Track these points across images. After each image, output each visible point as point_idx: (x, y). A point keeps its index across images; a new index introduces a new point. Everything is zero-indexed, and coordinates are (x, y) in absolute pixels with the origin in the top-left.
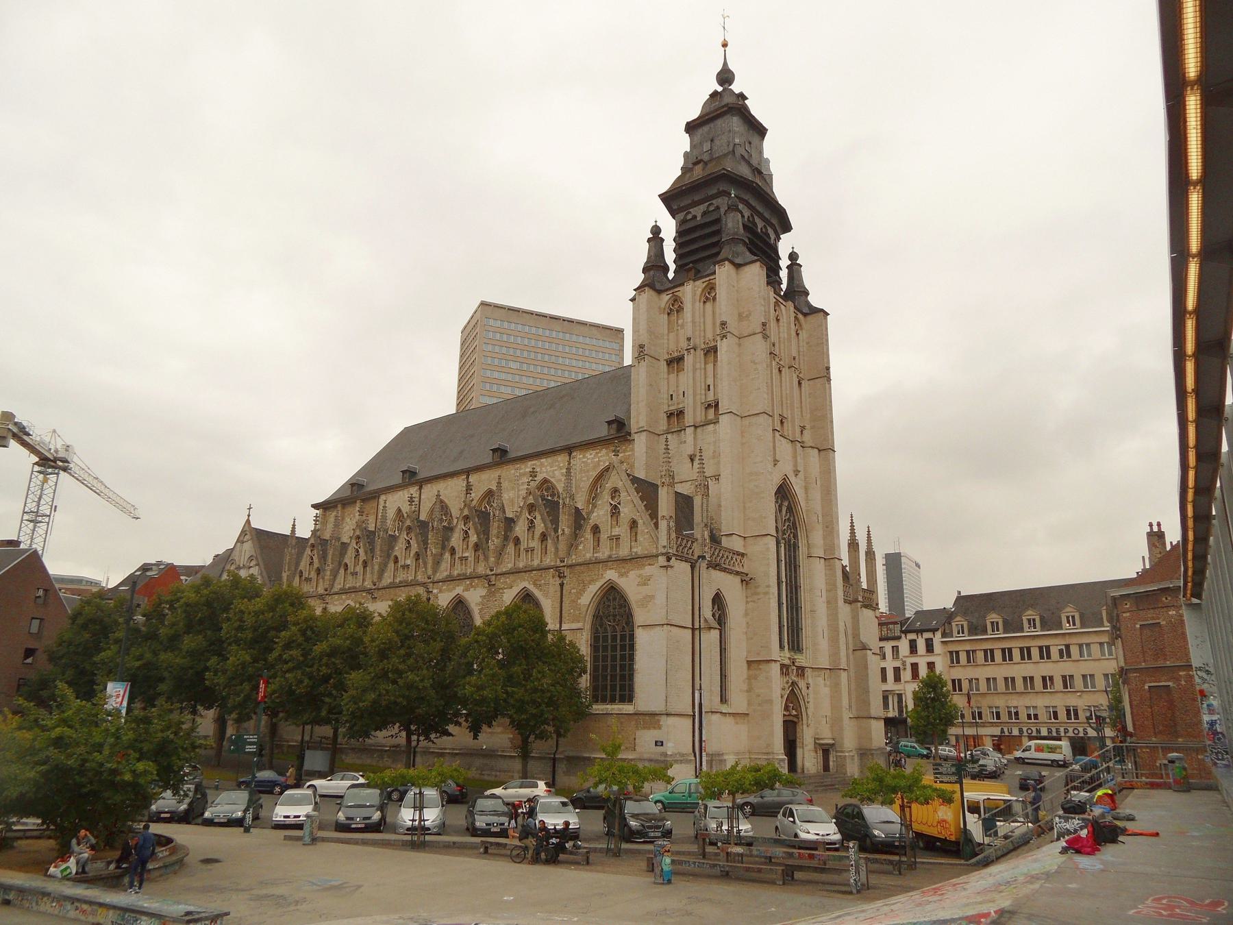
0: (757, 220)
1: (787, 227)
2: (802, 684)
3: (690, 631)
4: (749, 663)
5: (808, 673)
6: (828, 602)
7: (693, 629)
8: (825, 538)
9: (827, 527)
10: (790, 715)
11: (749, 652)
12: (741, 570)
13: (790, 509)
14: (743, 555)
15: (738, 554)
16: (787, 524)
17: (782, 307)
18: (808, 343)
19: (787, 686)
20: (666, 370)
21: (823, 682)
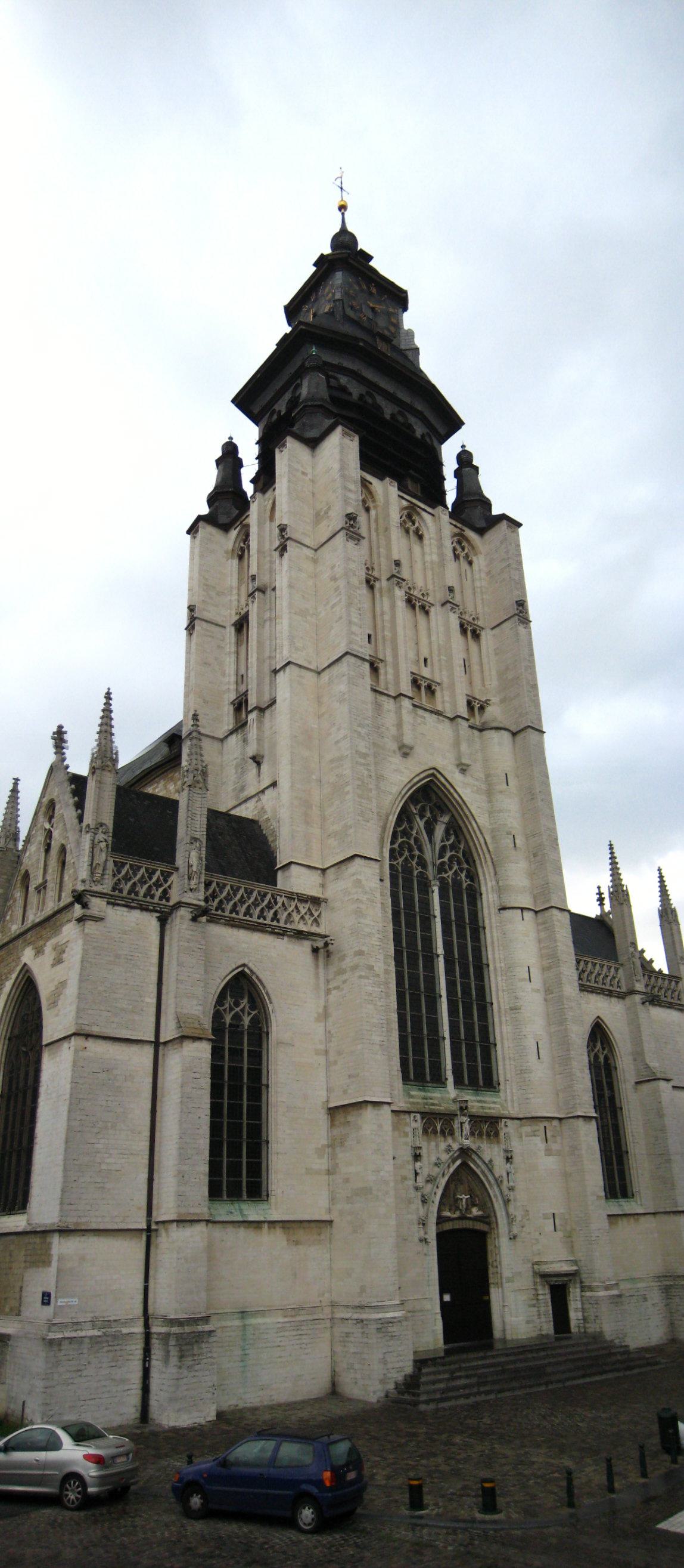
0: (380, 401)
1: (453, 423)
2: (490, 1152)
3: (149, 1051)
4: (333, 1112)
5: (508, 1129)
6: (548, 991)
7: (157, 1044)
8: (531, 875)
9: (535, 855)
10: (463, 1218)
11: (329, 1090)
12: (314, 929)
13: (456, 829)
14: (316, 901)
15: (303, 899)
16: (448, 854)
17: (424, 514)
18: (488, 573)
19: (445, 1157)
20: (233, 639)
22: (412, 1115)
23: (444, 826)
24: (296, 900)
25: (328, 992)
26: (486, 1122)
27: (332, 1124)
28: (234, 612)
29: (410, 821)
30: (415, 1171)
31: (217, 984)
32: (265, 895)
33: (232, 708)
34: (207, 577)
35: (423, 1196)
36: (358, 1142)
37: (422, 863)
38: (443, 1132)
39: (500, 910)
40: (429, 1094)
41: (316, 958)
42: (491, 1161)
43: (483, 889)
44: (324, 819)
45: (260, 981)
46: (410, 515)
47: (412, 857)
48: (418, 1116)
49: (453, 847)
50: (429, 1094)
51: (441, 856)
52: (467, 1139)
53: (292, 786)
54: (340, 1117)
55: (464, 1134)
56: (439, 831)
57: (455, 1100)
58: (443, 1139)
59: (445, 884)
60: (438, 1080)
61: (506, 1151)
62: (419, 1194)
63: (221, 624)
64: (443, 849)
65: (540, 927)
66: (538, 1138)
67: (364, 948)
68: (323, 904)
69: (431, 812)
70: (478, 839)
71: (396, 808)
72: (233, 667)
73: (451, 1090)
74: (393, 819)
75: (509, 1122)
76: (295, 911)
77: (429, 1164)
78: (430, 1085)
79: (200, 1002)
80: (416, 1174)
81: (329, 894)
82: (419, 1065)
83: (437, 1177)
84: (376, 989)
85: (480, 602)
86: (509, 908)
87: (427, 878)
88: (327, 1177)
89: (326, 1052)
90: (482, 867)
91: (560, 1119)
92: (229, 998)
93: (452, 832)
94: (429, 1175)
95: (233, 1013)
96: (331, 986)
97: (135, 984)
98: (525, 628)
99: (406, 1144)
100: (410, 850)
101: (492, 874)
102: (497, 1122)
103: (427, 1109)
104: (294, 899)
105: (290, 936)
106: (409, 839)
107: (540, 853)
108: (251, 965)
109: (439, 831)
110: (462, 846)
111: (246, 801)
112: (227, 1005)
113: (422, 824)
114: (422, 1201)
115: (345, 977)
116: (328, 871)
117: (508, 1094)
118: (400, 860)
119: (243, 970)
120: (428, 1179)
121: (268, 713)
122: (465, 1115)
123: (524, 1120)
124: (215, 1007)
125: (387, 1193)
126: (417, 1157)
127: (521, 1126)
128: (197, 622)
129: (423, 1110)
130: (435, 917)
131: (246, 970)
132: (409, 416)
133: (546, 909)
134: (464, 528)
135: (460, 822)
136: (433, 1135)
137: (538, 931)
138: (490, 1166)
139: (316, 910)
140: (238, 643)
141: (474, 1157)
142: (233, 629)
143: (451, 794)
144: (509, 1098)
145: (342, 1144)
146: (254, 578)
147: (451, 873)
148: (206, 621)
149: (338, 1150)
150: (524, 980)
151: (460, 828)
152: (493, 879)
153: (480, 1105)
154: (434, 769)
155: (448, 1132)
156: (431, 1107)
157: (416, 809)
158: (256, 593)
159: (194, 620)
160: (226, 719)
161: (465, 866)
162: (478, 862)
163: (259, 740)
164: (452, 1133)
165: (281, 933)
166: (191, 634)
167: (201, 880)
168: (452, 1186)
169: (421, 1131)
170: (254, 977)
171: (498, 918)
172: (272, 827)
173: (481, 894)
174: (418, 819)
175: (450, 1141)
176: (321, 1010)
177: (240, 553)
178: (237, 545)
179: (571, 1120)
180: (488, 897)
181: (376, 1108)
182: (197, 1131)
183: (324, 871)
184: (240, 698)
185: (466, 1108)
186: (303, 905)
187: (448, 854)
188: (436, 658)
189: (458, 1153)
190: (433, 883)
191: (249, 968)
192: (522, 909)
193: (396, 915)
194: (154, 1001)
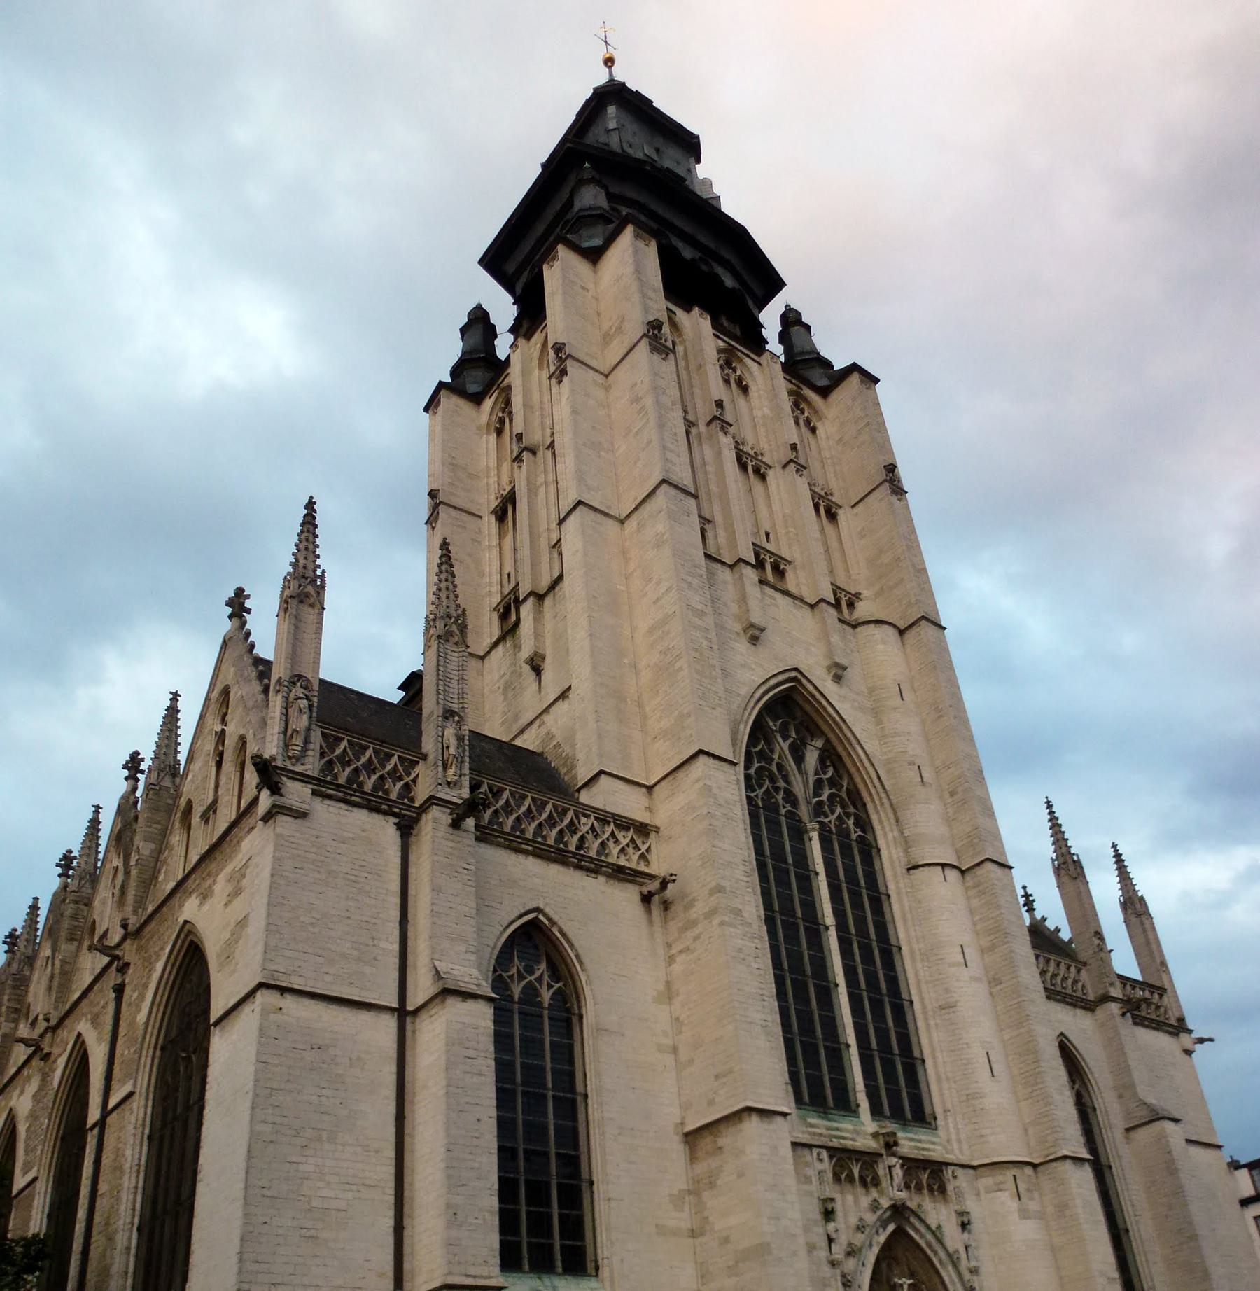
1: (772, 283)
2: (938, 1214)
4: (692, 1138)
5: (959, 1182)
7: (404, 1014)
11: (685, 1106)
13: (830, 756)
14: (643, 830)
19: (871, 1218)
21: (1013, 1205)
22: (815, 1151)
23: (816, 754)
24: (612, 824)
25: (671, 960)
26: (925, 1169)
27: (693, 1158)
28: (493, 497)
29: (769, 742)
30: (829, 1236)
31: (497, 936)
32: (565, 811)
33: (495, 616)
34: (454, 455)
35: (843, 1276)
36: (741, 1175)
37: (790, 797)
38: (864, 1183)
39: (909, 869)
40: (836, 1125)
41: (649, 911)
42: (939, 1227)
43: (881, 843)
44: (644, 717)
45: (563, 934)
46: (728, 361)
47: (777, 789)
48: (825, 1154)
49: (833, 783)
50: (836, 1125)
51: (817, 793)
52: (901, 1191)
53: (594, 668)
54: (706, 1143)
55: (895, 1185)
56: (811, 758)
57: (875, 1135)
58: (864, 1191)
59: (827, 831)
60: (845, 1105)
61: (960, 1214)
62: (838, 1272)
63: (477, 513)
64: (819, 784)
65: (971, 893)
66: (1007, 1194)
67: (726, 884)
68: (653, 835)
69: (797, 733)
70: (868, 773)
71: (750, 714)
72: (496, 564)
73: (867, 1123)
74: (745, 730)
75: (959, 1172)
76: (611, 841)
77: (848, 1227)
78: (834, 1112)
79: (472, 949)
80: (830, 1240)
81: (659, 819)
82: (816, 1084)
83: (862, 1247)
84: (747, 943)
85: (833, 475)
86: (923, 866)
87: (800, 821)
88: (691, 1240)
89: (675, 1050)
90: (877, 812)
91: (1035, 1166)
92: (516, 959)
93: (828, 764)
94: (850, 1244)
95: (524, 983)
96: (673, 951)
97: (365, 918)
98: (900, 500)
99: (811, 1194)
100: (773, 780)
101: (893, 821)
102: (942, 1171)
103: (835, 1143)
104: (609, 823)
105: (609, 876)
106: (770, 764)
107: (960, 789)
108: (547, 910)
109: (811, 758)
110: (845, 784)
111: (522, 731)
112: (514, 971)
113: (785, 746)
114: (844, 1285)
115: (696, 931)
116: (657, 788)
117: (952, 1130)
118: (760, 792)
119: (537, 918)
120: (849, 1250)
121: (548, 601)
122: (894, 1155)
123: (982, 1169)
124: (495, 971)
125: (795, 1254)
126: (828, 1215)
127: (977, 1178)
128: (443, 512)
129: (831, 1144)
130: (817, 874)
131: (541, 917)
132: (715, 265)
133: (978, 864)
134: (801, 386)
135: (840, 749)
136: (848, 1186)
137: (968, 898)
138: (938, 1235)
139: (643, 843)
140: (501, 535)
141: (912, 1219)
142: (493, 518)
143: (825, 709)
144: (953, 1137)
145: (712, 1185)
146: (519, 437)
147: (833, 818)
148: (455, 508)
149: (706, 1195)
150: (957, 964)
151: (840, 758)
152: (894, 827)
153: (913, 1144)
154: (796, 669)
155: (870, 1181)
156: (842, 1141)
157: (775, 725)
158: (524, 453)
159: (437, 507)
160: (487, 630)
161: (852, 810)
162: (870, 806)
163: (538, 636)
164: (876, 1183)
165: (594, 868)
166: (433, 528)
167: (463, 772)
168: (884, 1266)
169: (830, 1175)
170: (555, 930)
171: (906, 881)
172: (564, 754)
173: (879, 850)
174: (780, 740)
175: (874, 1193)
176: (661, 987)
177: (498, 426)
178: (494, 417)
179: (1054, 1164)
180: (890, 853)
181: (766, 1120)
182: (476, 1142)
183: (650, 789)
184: (506, 599)
185: (896, 1144)
186: (623, 833)
187: (826, 793)
188: (781, 531)
189: (888, 1213)
190: (809, 827)
191: (545, 915)
192: (943, 865)
193: (761, 866)
194: (396, 947)
